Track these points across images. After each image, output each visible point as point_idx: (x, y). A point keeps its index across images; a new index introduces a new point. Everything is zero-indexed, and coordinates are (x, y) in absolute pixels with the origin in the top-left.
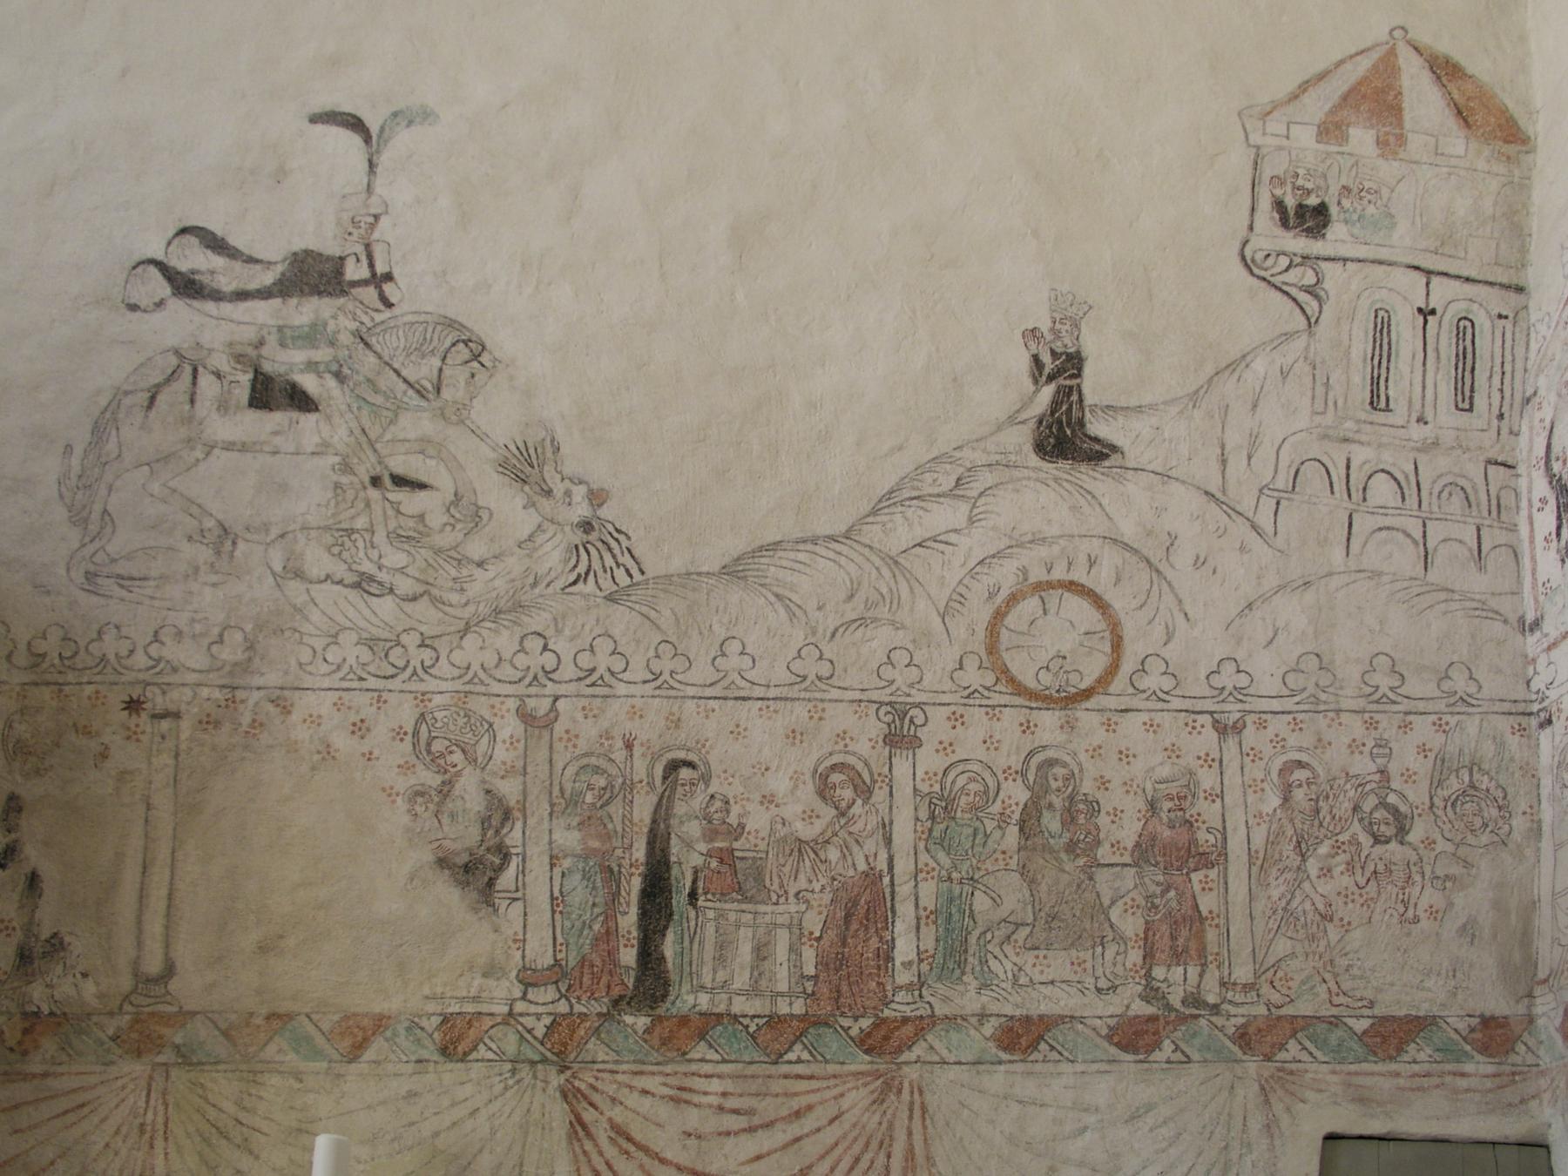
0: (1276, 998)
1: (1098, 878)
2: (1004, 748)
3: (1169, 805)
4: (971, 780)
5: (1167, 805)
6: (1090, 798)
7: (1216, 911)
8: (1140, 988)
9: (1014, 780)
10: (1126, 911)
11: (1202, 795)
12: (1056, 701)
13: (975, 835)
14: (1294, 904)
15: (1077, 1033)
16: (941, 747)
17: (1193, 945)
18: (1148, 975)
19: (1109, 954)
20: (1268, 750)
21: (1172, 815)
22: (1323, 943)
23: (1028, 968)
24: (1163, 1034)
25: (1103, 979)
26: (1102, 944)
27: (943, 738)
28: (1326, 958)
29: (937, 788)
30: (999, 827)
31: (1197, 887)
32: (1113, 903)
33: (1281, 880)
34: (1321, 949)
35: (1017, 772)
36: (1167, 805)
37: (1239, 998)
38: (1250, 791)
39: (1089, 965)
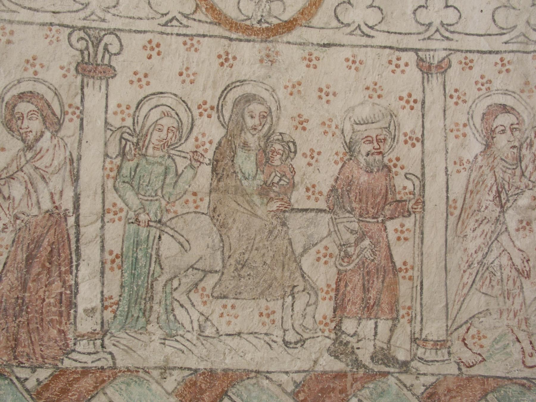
0: (467, 356)
1: (291, 223)
2: (201, 80)
3: (368, 147)
4: (165, 115)
5: (366, 148)
6: (287, 138)
7: (410, 262)
8: (329, 342)
9: (209, 116)
10: (318, 259)
11: (402, 138)
12: (257, 32)
13: (166, 174)
14: (491, 257)
15: (262, 389)
16: (135, 78)
17: (385, 298)
18: (338, 328)
19: (299, 305)
20: (472, 93)
21: (370, 158)
22: (518, 301)
23: (215, 318)
24: (350, 391)
25: (292, 332)
26: (293, 295)
27: (138, 69)
28: (521, 316)
29: (129, 122)
30: (191, 166)
31: (392, 236)
32: (305, 250)
33: (479, 232)
34: (517, 306)
35: (212, 108)
36: (366, 148)
37: (430, 355)
38: (451, 136)
39: (277, 316)
